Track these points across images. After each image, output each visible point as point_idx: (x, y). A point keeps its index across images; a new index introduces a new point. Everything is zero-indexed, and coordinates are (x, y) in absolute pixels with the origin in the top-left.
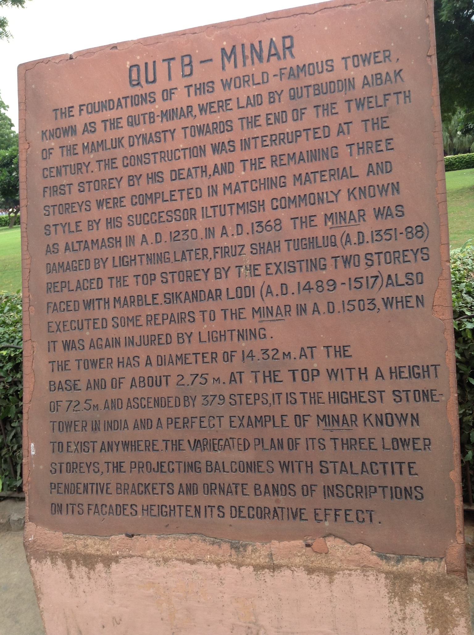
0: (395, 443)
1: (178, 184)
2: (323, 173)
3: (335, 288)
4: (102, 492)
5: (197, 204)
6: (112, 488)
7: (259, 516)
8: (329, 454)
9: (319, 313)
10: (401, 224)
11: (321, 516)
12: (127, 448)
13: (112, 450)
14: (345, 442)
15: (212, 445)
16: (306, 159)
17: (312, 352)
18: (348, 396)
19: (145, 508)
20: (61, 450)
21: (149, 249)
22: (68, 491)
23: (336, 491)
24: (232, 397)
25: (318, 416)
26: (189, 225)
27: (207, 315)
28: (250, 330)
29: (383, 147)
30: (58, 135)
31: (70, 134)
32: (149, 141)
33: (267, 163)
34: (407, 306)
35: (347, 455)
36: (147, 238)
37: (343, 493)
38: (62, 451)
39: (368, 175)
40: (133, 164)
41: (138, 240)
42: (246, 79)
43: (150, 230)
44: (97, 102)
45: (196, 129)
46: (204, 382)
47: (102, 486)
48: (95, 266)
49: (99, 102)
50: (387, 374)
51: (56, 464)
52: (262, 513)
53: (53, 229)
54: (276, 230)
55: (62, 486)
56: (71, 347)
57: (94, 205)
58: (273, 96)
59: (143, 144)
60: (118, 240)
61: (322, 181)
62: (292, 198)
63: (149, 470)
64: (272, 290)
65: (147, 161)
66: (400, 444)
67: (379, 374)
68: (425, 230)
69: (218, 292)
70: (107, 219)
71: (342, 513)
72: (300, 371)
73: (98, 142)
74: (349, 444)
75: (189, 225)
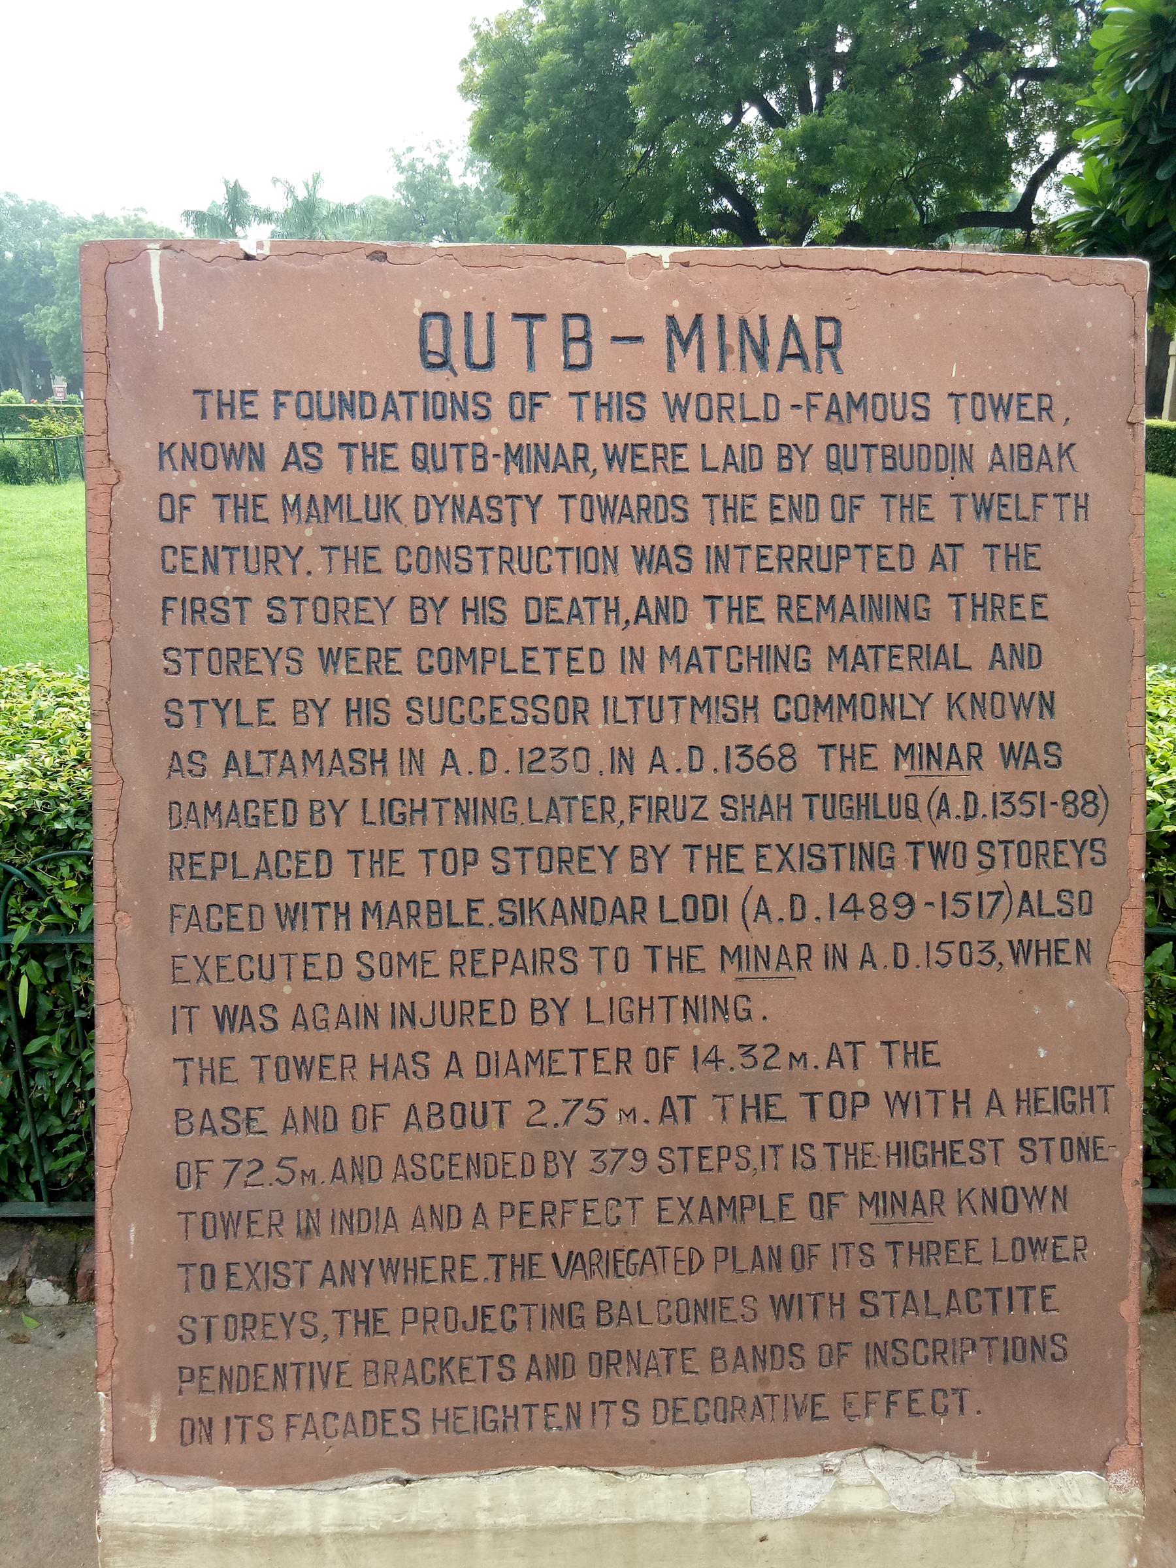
2: (896, 651)
3: (911, 911)
4: (325, 1383)
5: (591, 687)
6: (353, 1372)
7: (721, 1416)
8: (880, 1278)
9: (874, 966)
10: (1053, 783)
11: (858, 1408)
12: (395, 1274)
13: (352, 1281)
14: (916, 1249)
15: (612, 1263)
17: (855, 1052)
20: (208, 1284)
21: (464, 787)
22: (230, 1383)
23: (891, 1353)
24: (665, 1153)
26: (570, 735)
27: (608, 958)
28: (714, 998)
29: (1025, 610)
30: (209, 461)
31: (245, 464)
32: (471, 515)
34: (1058, 961)
35: (918, 1277)
36: (458, 758)
37: (906, 1358)
38: (213, 1286)
39: (992, 667)
40: (424, 567)
41: (433, 761)
42: (726, 402)
43: (469, 740)
44: (326, 390)
45: (596, 504)
46: (595, 1120)
47: (324, 1369)
48: (312, 817)
50: (1009, 1103)
51: (194, 1320)
52: (726, 1409)
53: (189, 712)
54: (782, 769)
55: (215, 1375)
57: (312, 662)
58: (789, 456)
59: (454, 520)
60: (378, 756)
61: (892, 668)
63: (451, 1326)
64: (770, 906)
65: (464, 565)
66: (1028, 1249)
67: (995, 1104)
68: (1101, 801)
69: (639, 903)
70: (348, 700)
72: (826, 1096)
73: (326, 497)
74: (923, 1252)
75: (570, 735)
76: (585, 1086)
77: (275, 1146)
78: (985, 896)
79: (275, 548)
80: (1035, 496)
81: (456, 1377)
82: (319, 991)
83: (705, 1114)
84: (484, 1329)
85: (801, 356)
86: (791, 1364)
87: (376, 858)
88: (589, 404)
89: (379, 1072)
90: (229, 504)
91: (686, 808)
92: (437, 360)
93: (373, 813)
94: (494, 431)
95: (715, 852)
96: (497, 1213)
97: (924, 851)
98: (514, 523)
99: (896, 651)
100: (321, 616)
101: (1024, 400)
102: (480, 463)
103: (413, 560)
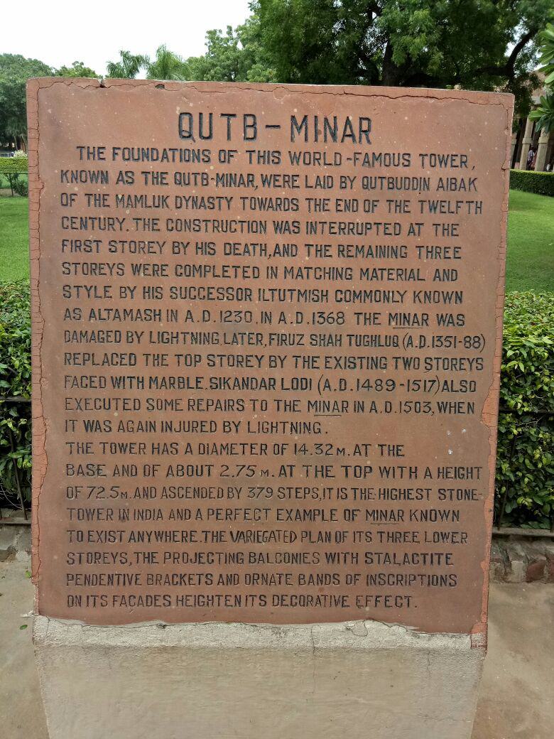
0: (436, 536)
1: (232, 260)
2: (391, 271)
3: (394, 388)
4: (130, 584)
6: (142, 579)
7: (302, 603)
8: (375, 546)
10: (461, 333)
12: (161, 538)
13: (143, 540)
14: (391, 535)
16: (374, 253)
18: (397, 493)
19: (180, 598)
21: (195, 328)
22: (89, 582)
23: (378, 580)
24: (281, 490)
25: (367, 511)
26: (243, 306)
27: (258, 405)
28: (304, 423)
29: (451, 254)
30: (83, 179)
32: (200, 206)
33: (333, 251)
35: (391, 548)
38: (82, 540)
40: (179, 229)
41: (182, 315)
42: (317, 156)
43: (197, 307)
44: (136, 147)
45: (257, 202)
47: (130, 578)
48: (127, 339)
49: (139, 149)
50: (435, 474)
51: (74, 554)
52: (305, 601)
53: (74, 291)
54: (338, 323)
56: (94, 429)
57: (128, 270)
59: (193, 208)
60: (157, 313)
61: (389, 279)
62: (358, 293)
63: (185, 561)
65: (197, 228)
66: (441, 537)
67: (428, 474)
68: (482, 341)
69: (272, 381)
70: (144, 287)
71: (382, 600)
73: (136, 196)
74: (394, 537)
76: (248, 459)
77: (108, 482)
78: (427, 382)
79: (113, 219)
80: (457, 202)
81: (187, 583)
82: (128, 416)
83: (299, 474)
84: (200, 563)
85: (352, 135)
86: (334, 583)
87: (156, 357)
88: (255, 156)
89: (156, 451)
90: (92, 199)
91: (295, 340)
92: (187, 135)
93: (155, 338)
94: (212, 168)
95: (307, 360)
96: (206, 513)
97: (400, 361)
98: (220, 209)
99: (391, 271)
100: (133, 250)
101: (454, 158)
102: (205, 182)
103: (174, 225)
